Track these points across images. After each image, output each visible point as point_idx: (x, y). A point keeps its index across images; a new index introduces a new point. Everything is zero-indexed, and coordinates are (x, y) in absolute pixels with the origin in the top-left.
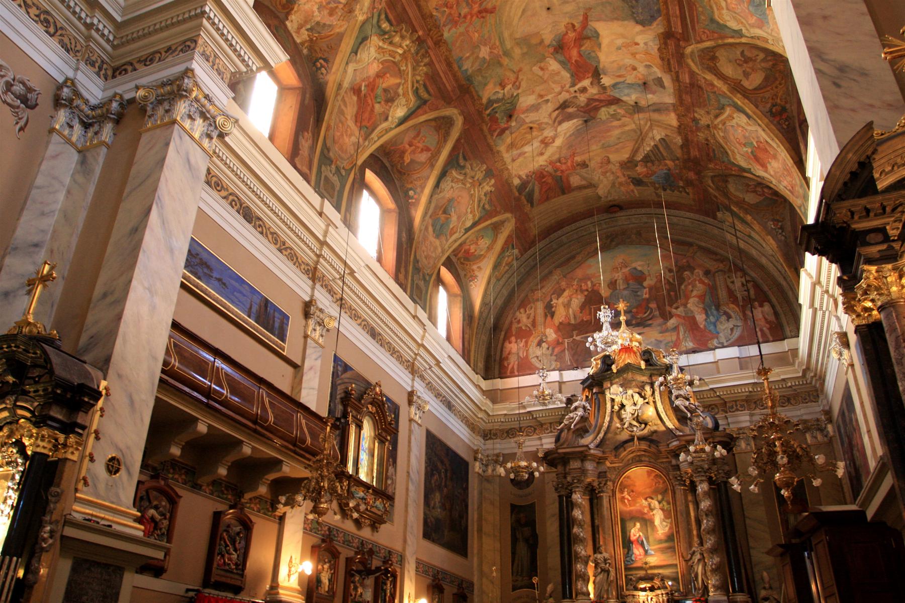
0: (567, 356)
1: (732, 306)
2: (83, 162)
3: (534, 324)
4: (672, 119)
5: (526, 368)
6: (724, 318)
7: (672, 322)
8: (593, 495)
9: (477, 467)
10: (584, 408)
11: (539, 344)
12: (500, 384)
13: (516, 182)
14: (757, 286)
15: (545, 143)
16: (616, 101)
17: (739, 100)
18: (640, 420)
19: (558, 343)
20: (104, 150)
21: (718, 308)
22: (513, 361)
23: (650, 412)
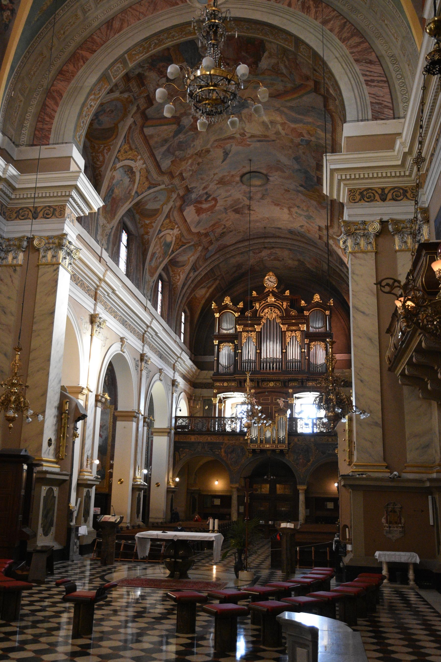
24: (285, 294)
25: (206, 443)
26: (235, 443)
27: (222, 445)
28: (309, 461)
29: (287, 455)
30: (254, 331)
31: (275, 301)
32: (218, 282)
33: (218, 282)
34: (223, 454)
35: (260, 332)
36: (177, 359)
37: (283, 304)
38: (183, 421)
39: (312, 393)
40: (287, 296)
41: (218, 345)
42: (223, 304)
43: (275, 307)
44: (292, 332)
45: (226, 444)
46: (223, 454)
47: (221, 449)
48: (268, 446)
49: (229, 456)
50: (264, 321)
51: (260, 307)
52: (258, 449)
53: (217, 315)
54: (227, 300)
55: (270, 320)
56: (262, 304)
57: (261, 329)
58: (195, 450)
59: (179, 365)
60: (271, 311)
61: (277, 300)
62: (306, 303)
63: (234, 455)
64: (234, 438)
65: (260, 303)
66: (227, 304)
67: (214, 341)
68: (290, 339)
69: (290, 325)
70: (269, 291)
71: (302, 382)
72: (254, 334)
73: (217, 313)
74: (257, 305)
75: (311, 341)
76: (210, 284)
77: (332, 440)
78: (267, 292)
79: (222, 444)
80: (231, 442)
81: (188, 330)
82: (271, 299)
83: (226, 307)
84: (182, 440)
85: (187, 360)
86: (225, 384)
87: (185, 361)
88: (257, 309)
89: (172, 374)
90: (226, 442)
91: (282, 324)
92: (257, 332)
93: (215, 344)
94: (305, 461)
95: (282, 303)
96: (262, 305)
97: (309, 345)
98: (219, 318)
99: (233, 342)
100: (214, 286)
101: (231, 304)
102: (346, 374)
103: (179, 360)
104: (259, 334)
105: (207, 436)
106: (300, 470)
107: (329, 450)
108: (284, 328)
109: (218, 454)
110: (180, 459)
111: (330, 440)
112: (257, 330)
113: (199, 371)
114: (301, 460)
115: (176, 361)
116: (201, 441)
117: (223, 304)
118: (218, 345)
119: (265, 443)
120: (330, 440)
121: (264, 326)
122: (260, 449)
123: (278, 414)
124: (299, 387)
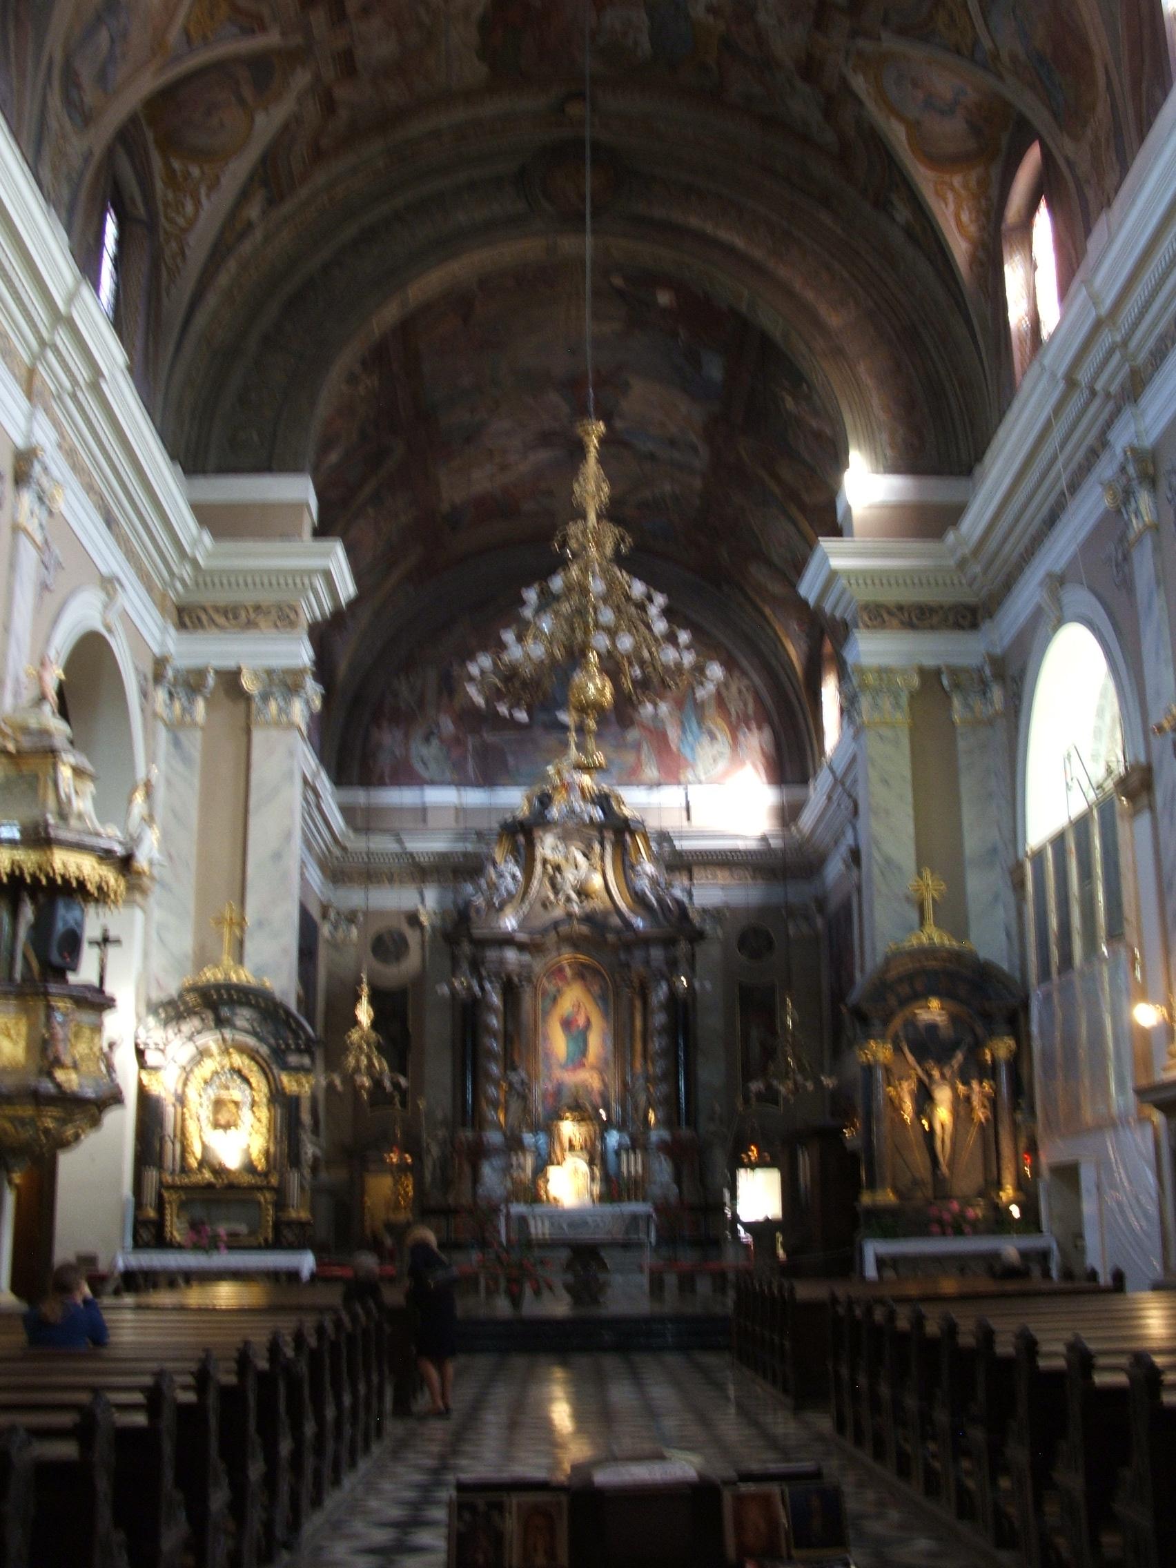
0: (470, 766)
1: (719, 721)
2: (176, 743)
3: (421, 703)
4: (698, 483)
5: (405, 776)
6: (705, 739)
7: (633, 734)
8: (511, 991)
9: (325, 930)
10: (514, 877)
11: (427, 739)
12: (360, 796)
13: (445, 507)
14: (758, 699)
15: (503, 468)
16: (626, 445)
17: (794, 511)
18: (583, 892)
19: (458, 741)
20: (198, 735)
21: (700, 723)
22: (384, 762)
23: (597, 881)
89: (22, 421)
103: (62, 338)
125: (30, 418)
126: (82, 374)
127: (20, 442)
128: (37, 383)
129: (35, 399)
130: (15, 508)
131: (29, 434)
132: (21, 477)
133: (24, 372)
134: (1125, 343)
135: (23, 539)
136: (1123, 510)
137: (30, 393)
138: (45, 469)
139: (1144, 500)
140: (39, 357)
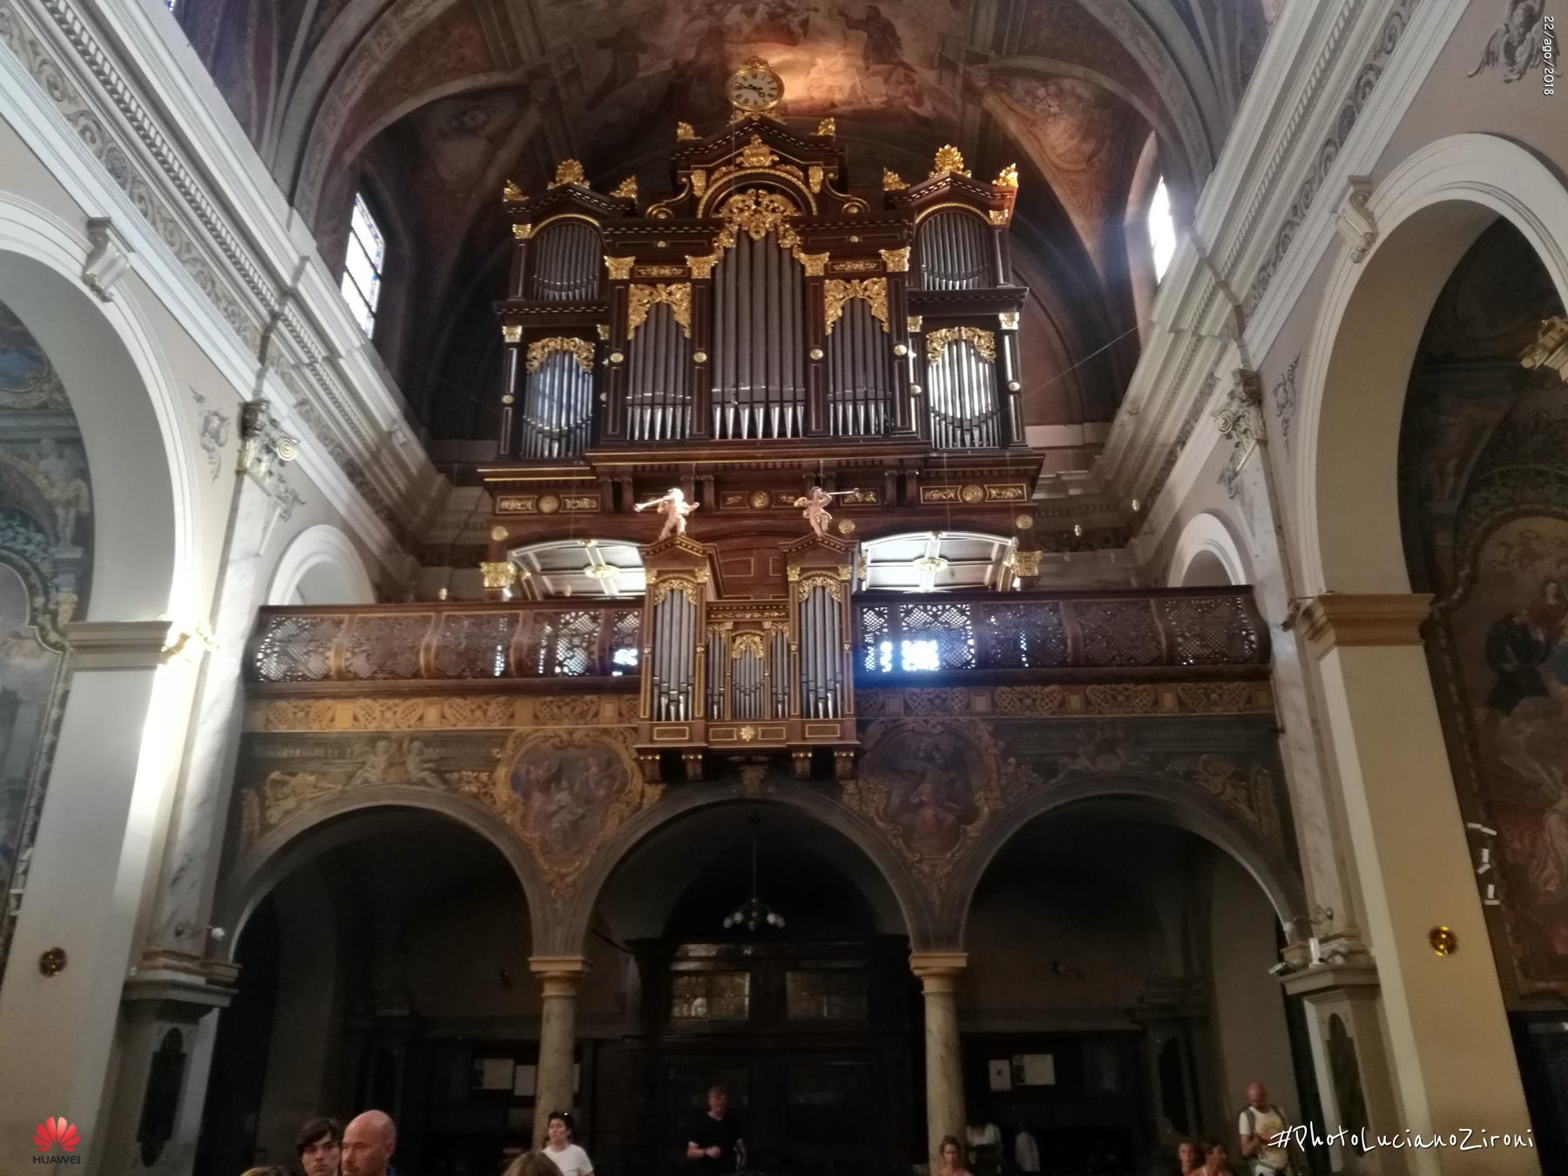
24: (817, 131)
25: (413, 739)
26: (571, 733)
27: (502, 745)
28: (970, 815)
29: (850, 787)
30: (686, 277)
31: (774, 165)
32: (533, 117)
33: (533, 117)
34: (502, 792)
35: (710, 284)
36: (282, 304)
37: (807, 177)
38: (302, 628)
39: (944, 534)
40: (826, 139)
41: (523, 347)
42: (550, 187)
43: (771, 190)
44: (848, 281)
45: (521, 739)
46: (502, 792)
47: (492, 764)
48: (746, 733)
49: (537, 799)
50: (726, 241)
51: (707, 187)
52: (695, 750)
53: (522, 231)
54: (572, 174)
55: (752, 242)
56: (716, 175)
57: (713, 270)
58: (350, 777)
59: (306, 360)
60: (757, 203)
61: (784, 161)
62: (903, 180)
63: (563, 797)
64: (566, 710)
65: (710, 172)
66: (569, 185)
67: (504, 332)
68: (843, 308)
69: (842, 253)
70: (749, 121)
71: (901, 482)
72: (679, 297)
73: (521, 222)
74: (698, 180)
75: (931, 325)
76: (499, 120)
77: (1088, 703)
78: (740, 127)
79: (500, 739)
80: (550, 728)
81: (401, 307)
82: (758, 157)
83: (565, 199)
84: (282, 729)
85: (349, 352)
86: (548, 505)
87: (343, 352)
88: (698, 193)
89: (252, 380)
90: (522, 727)
91: (808, 249)
92: (695, 283)
93: (507, 340)
94: (951, 818)
95: (805, 169)
96: (717, 180)
97: (921, 343)
98: (530, 242)
99: (589, 335)
100: (518, 138)
101: (587, 186)
102: (1073, 492)
103: (290, 310)
104: (704, 295)
105: (420, 701)
106: (926, 868)
107: (1075, 756)
108: (814, 265)
109: (476, 796)
110: (266, 827)
111: (1075, 702)
112: (695, 274)
113: (440, 479)
114: (928, 813)
115: (275, 316)
116: (388, 727)
117: (550, 187)
118: (523, 347)
119: (734, 717)
120: (1075, 702)
121: (725, 261)
122: (704, 751)
123: (803, 570)
124: (885, 509)
125: (260, 376)
126: (319, 352)
127: (249, 398)
128: (271, 351)
129: (267, 363)
130: (242, 452)
131: (257, 392)
132: (247, 424)
133: (258, 342)
134: (1223, 284)
135: (247, 479)
136: (1234, 433)
137: (262, 358)
138: (273, 422)
139: (1251, 419)
140: (268, 329)
